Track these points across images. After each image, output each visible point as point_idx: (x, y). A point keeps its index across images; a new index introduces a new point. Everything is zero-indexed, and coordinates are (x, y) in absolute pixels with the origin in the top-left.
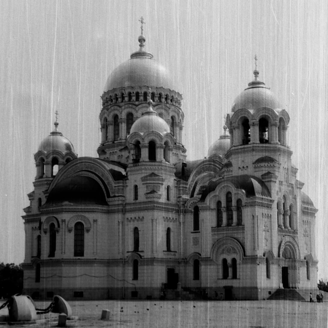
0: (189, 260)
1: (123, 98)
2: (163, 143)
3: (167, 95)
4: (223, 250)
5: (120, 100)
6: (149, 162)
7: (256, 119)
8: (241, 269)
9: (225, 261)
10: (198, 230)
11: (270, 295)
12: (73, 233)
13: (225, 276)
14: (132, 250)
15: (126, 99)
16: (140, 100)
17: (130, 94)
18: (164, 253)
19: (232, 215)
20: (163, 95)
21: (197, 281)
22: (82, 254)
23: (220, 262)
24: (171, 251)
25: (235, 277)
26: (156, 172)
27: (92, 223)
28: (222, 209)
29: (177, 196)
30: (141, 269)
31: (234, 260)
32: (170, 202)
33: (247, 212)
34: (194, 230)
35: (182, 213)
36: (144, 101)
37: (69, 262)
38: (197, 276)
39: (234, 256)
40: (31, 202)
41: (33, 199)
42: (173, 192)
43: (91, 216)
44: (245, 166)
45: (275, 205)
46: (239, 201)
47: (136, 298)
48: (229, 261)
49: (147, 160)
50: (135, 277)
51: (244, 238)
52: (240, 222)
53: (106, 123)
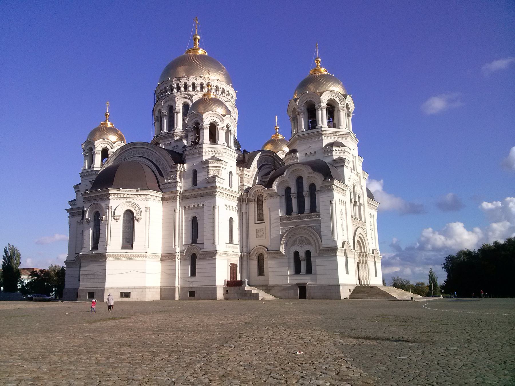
0: (253, 254)
1: (178, 88)
2: (225, 125)
3: (223, 89)
4: (295, 241)
5: (175, 90)
6: (210, 144)
7: (323, 102)
8: (318, 264)
9: (296, 254)
10: (263, 220)
11: (350, 293)
12: (121, 221)
13: (297, 271)
14: (190, 243)
15: (183, 89)
16: (196, 90)
17: (185, 84)
18: (226, 245)
19: (304, 202)
20: (219, 88)
21: (261, 278)
22: (131, 247)
23: (292, 255)
24: (232, 244)
25: (309, 271)
26: (217, 156)
27: (143, 210)
28: (291, 195)
29: (240, 185)
30: (199, 264)
31: (308, 253)
32: (232, 189)
33: (321, 199)
34: (258, 220)
35: (244, 202)
36: (200, 92)
37: (116, 256)
38: (261, 272)
39: (308, 248)
40: (77, 194)
41: (79, 191)
42: (236, 179)
43: (142, 203)
44: (313, 152)
45: (348, 193)
46: (312, 187)
47: (193, 298)
48: (302, 255)
49: (209, 142)
50: (193, 273)
51: (320, 226)
52: (314, 208)
53: (160, 115)
